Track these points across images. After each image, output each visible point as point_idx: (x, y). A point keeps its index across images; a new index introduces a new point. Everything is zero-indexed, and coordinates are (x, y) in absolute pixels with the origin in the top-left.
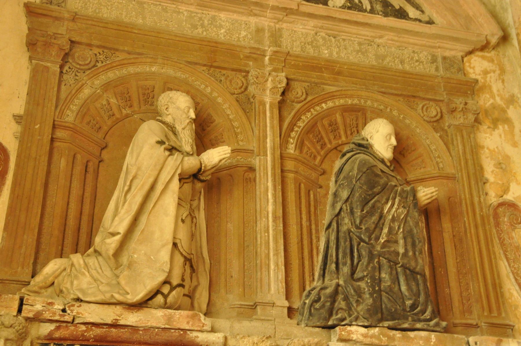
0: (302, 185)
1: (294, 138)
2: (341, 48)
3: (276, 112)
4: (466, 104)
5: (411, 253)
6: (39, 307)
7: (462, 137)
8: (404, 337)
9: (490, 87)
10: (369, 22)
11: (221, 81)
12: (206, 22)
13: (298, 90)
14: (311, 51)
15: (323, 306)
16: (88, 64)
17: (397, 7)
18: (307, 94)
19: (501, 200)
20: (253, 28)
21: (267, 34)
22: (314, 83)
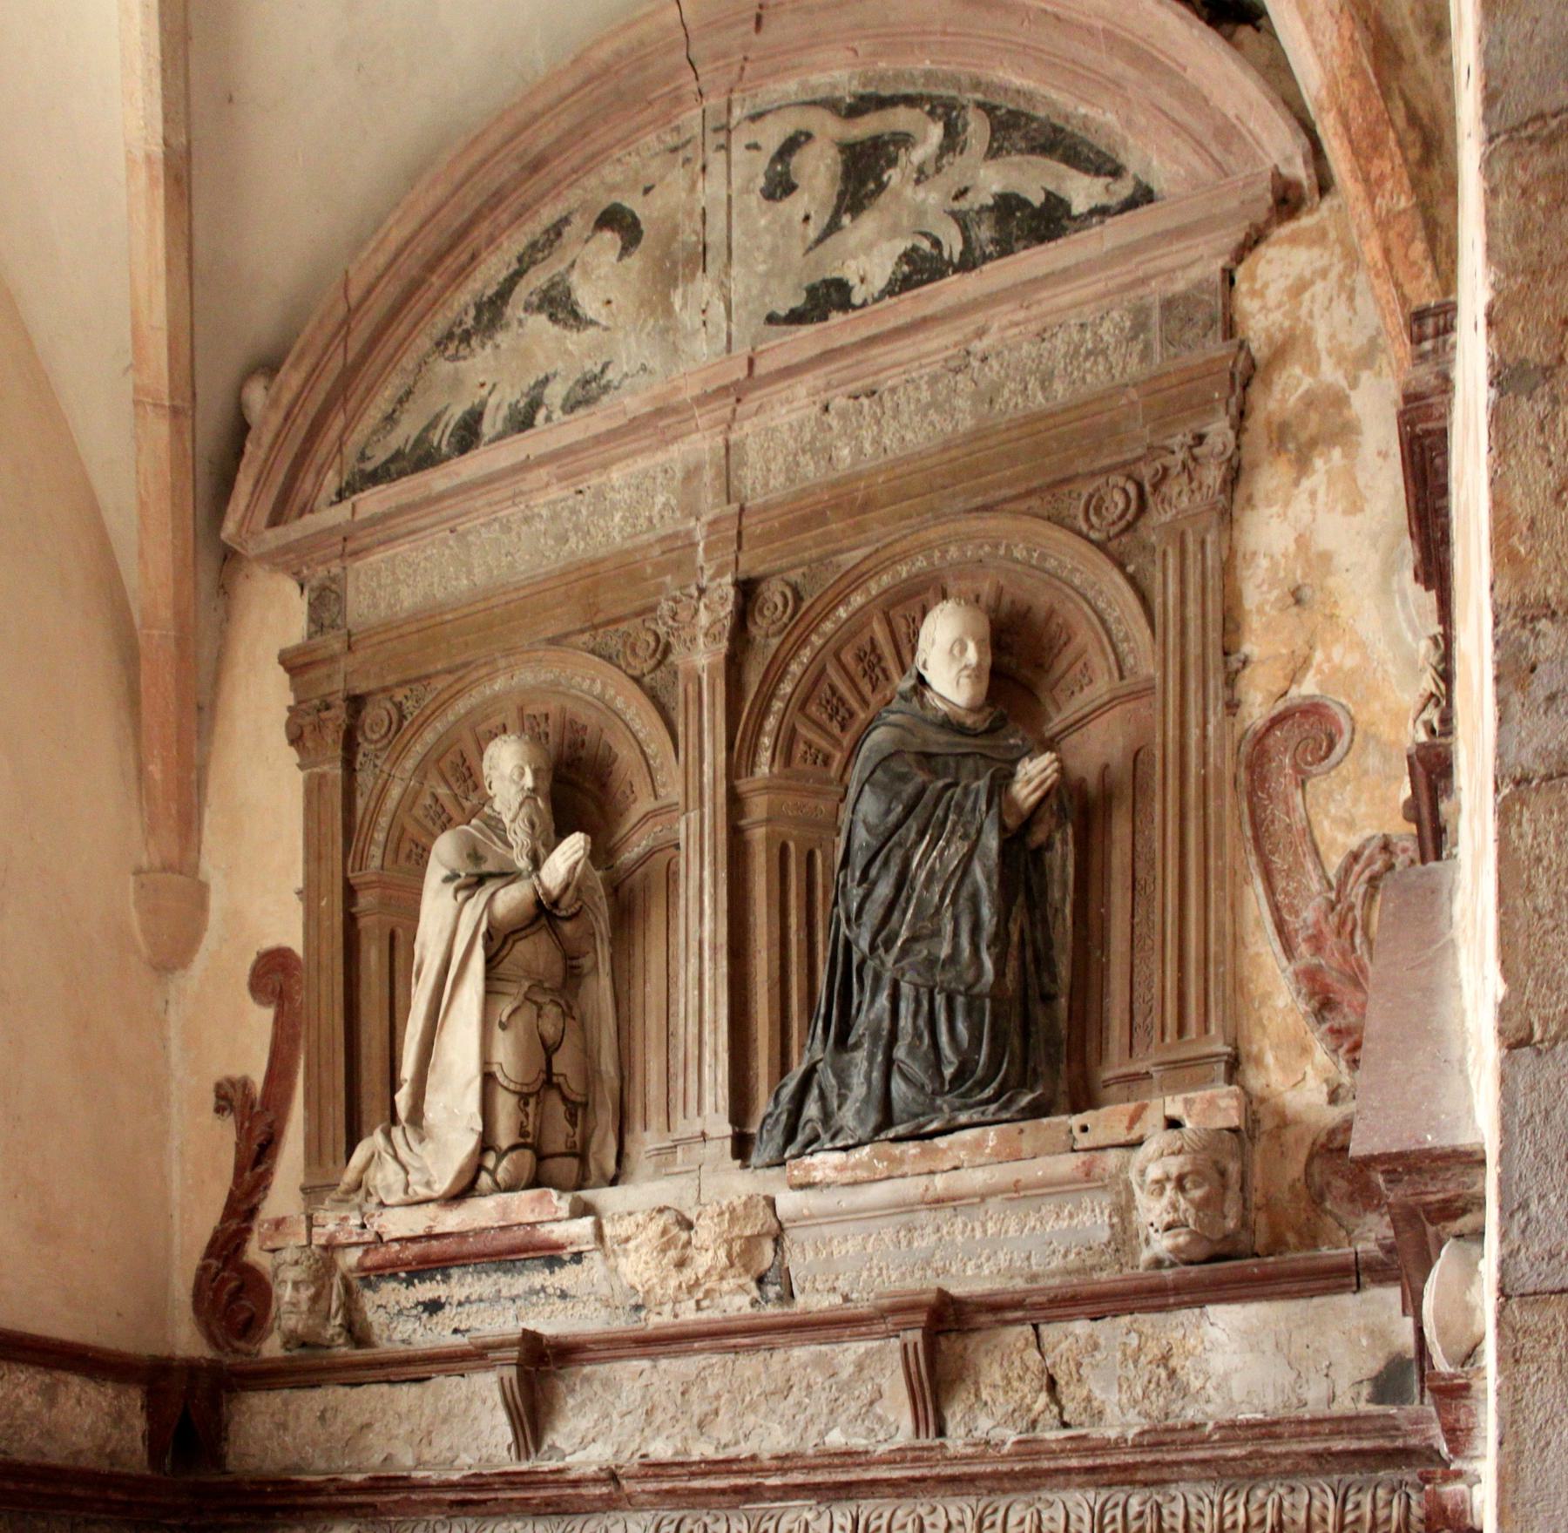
6: (331, 1227)
8: (923, 1153)
15: (777, 1120)
16: (391, 723)
22: (812, 561)
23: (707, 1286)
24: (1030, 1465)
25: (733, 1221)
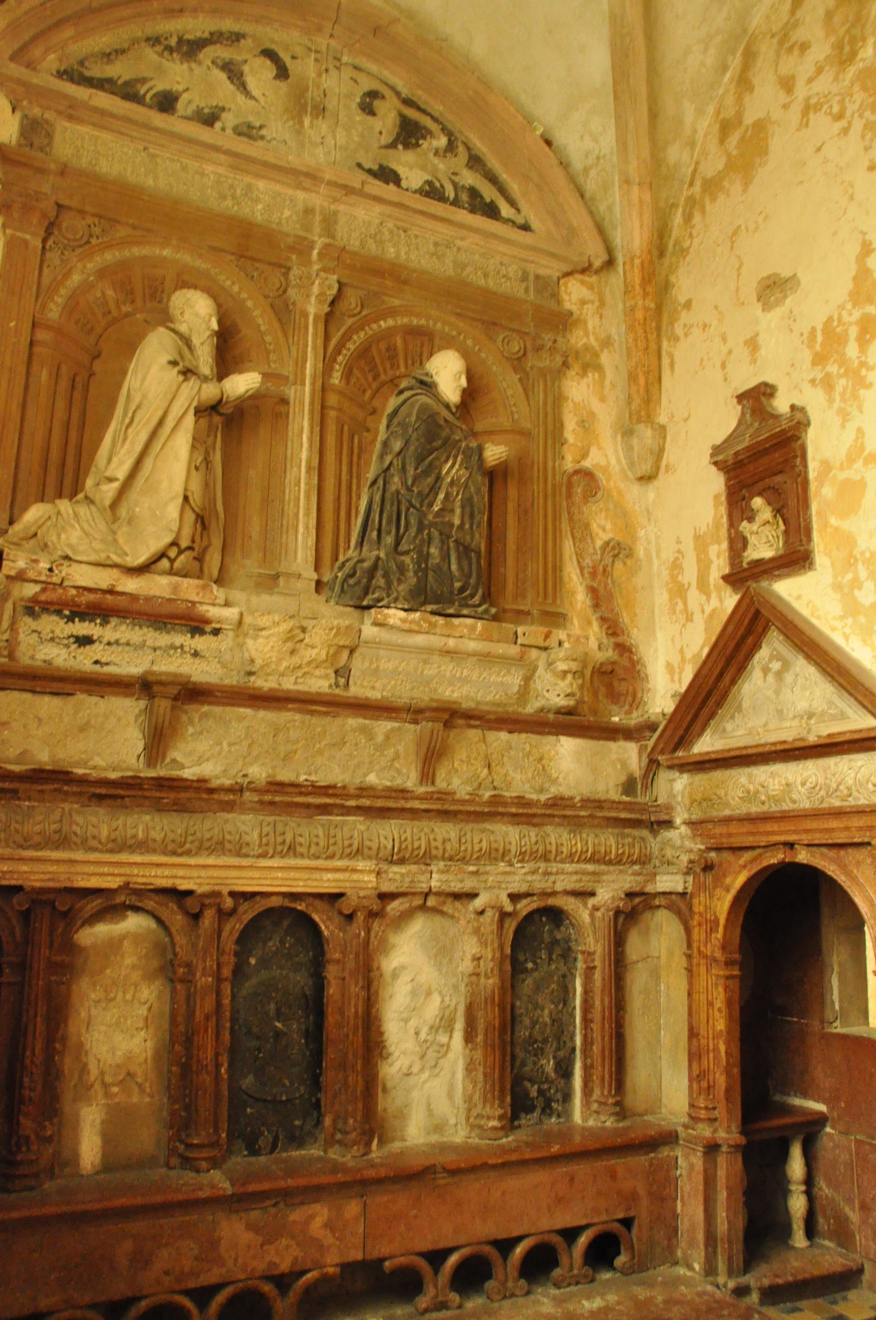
0: (346, 427)
1: (340, 364)
2: (412, 247)
3: (321, 327)
4: (555, 341)
5: (467, 526)
6: (21, 564)
7: (546, 385)
8: (447, 624)
9: (585, 322)
10: (451, 217)
11: (253, 277)
12: (239, 192)
13: (352, 299)
14: (372, 247)
15: (358, 583)
16: (79, 240)
17: (488, 200)
18: (362, 307)
19: (577, 467)
20: (300, 207)
21: (318, 218)
23: (306, 670)
24: (493, 809)
25: (336, 635)
